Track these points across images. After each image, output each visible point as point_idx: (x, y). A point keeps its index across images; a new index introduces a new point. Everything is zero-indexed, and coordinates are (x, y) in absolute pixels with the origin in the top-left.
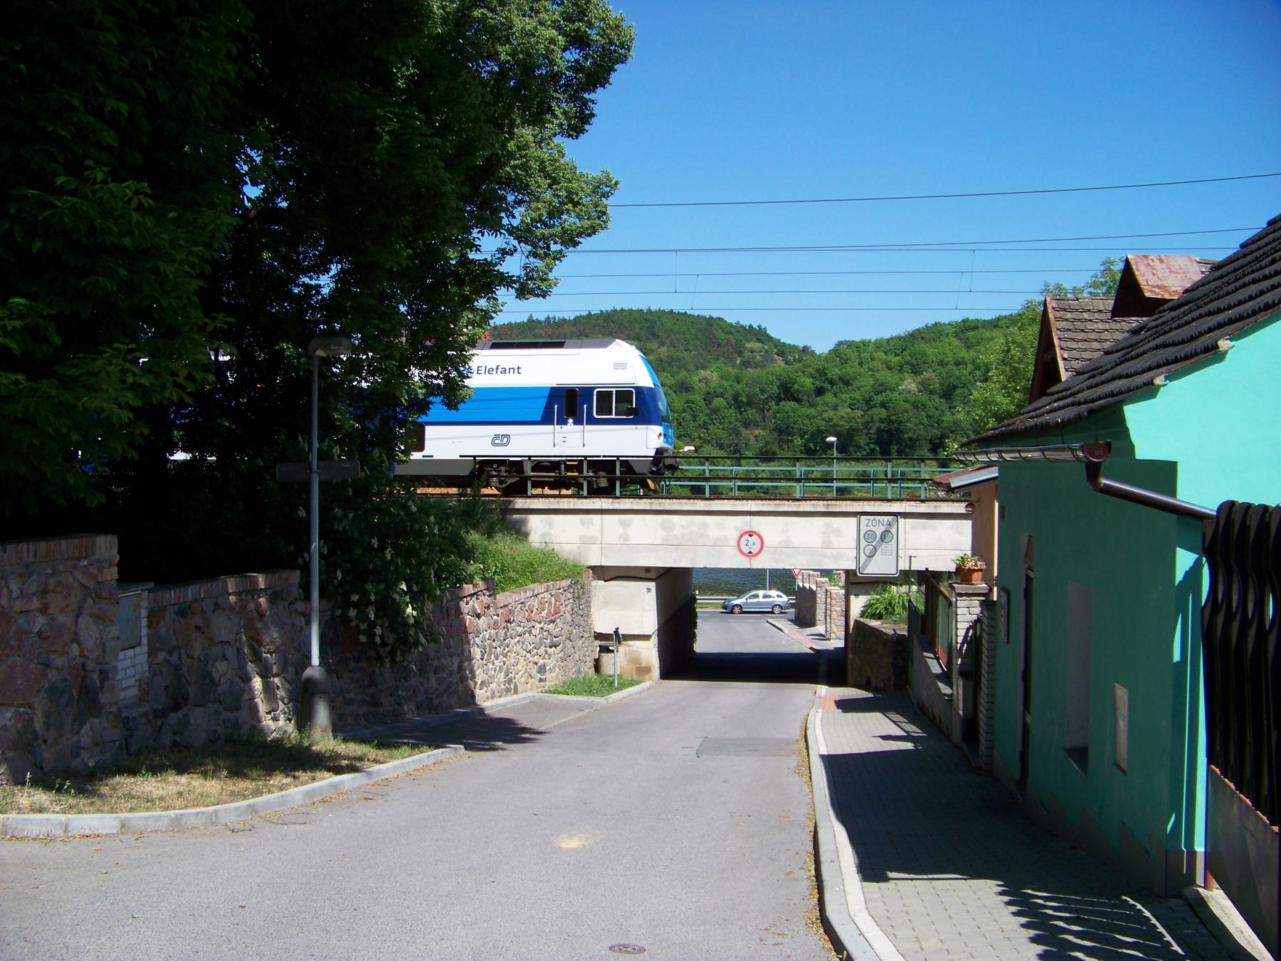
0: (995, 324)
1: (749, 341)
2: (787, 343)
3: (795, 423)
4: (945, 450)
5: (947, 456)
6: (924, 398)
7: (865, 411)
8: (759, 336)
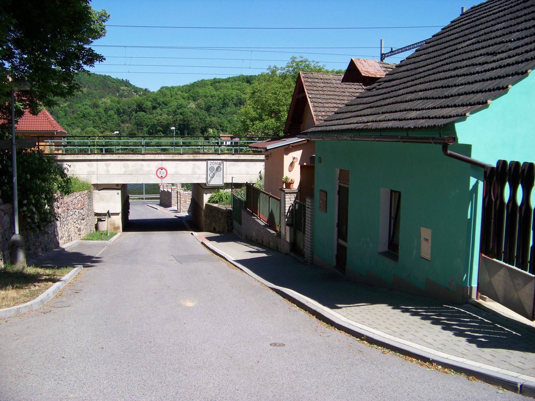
0: (227, 80)
1: (122, 86)
2: (138, 87)
3: (144, 121)
4: (207, 133)
5: (208, 135)
6: (198, 111)
7: (173, 116)
8: (126, 84)
